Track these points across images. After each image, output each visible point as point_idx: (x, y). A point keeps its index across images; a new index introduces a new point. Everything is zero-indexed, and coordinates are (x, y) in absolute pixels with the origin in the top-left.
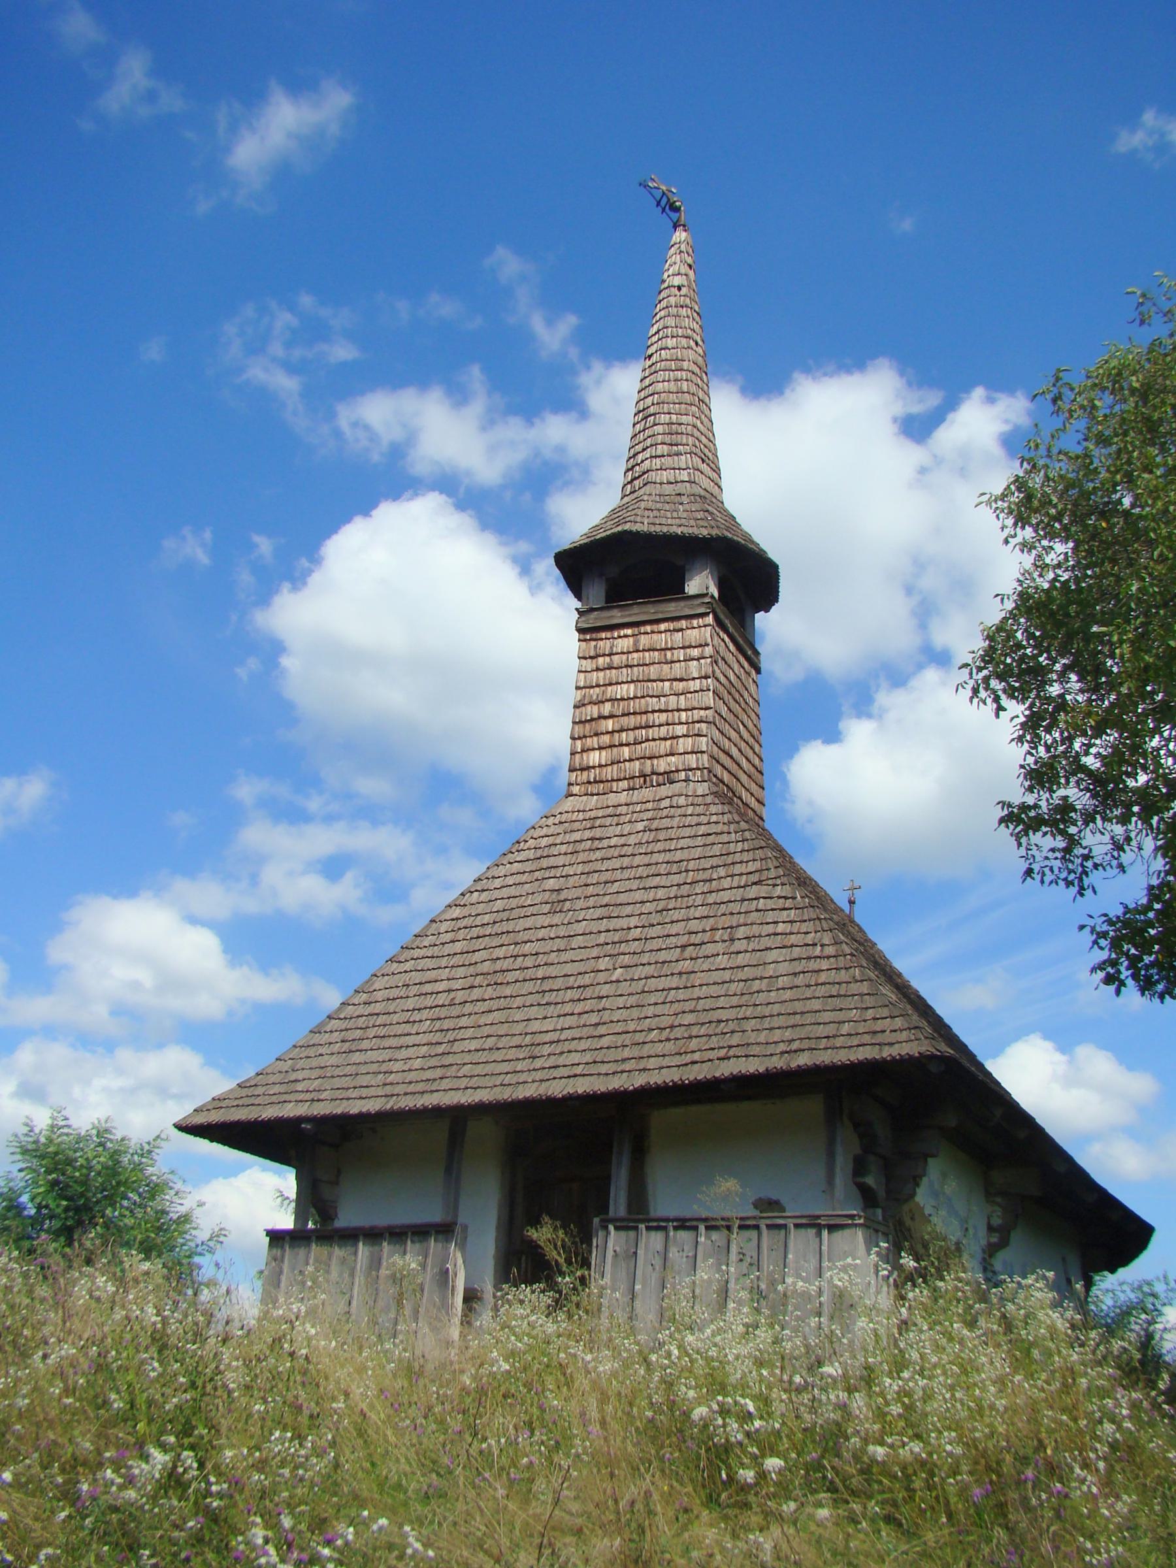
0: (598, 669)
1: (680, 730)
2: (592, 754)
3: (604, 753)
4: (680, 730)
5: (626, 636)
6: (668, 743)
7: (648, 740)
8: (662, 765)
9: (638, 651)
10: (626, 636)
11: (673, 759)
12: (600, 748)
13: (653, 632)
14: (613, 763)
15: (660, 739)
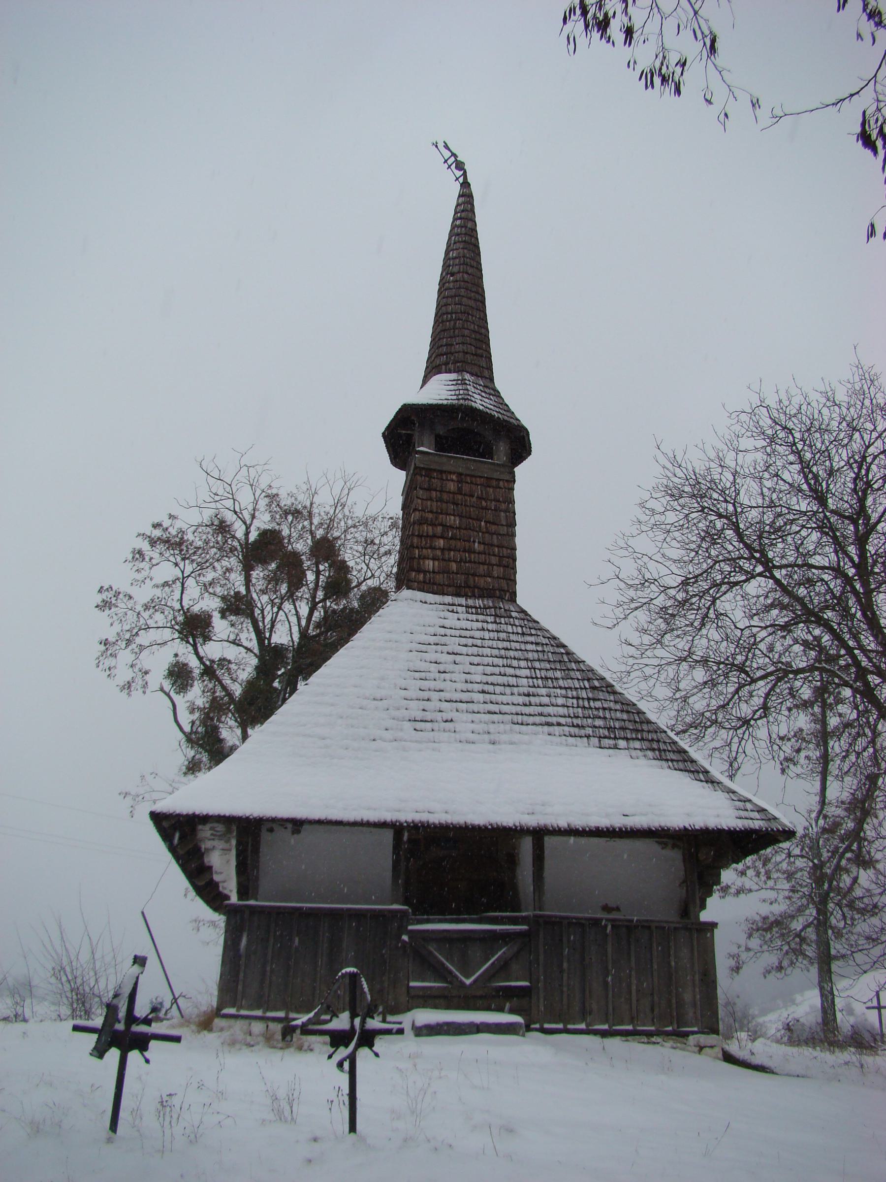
0: (431, 499)
1: (494, 560)
2: (427, 562)
3: (436, 563)
4: (494, 560)
5: (452, 480)
6: (486, 567)
7: (470, 562)
8: (481, 582)
9: (461, 494)
10: (452, 480)
11: (489, 580)
12: (434, 559)
13: (472, 483)
14: (444, 572)
15: (479, 563)
